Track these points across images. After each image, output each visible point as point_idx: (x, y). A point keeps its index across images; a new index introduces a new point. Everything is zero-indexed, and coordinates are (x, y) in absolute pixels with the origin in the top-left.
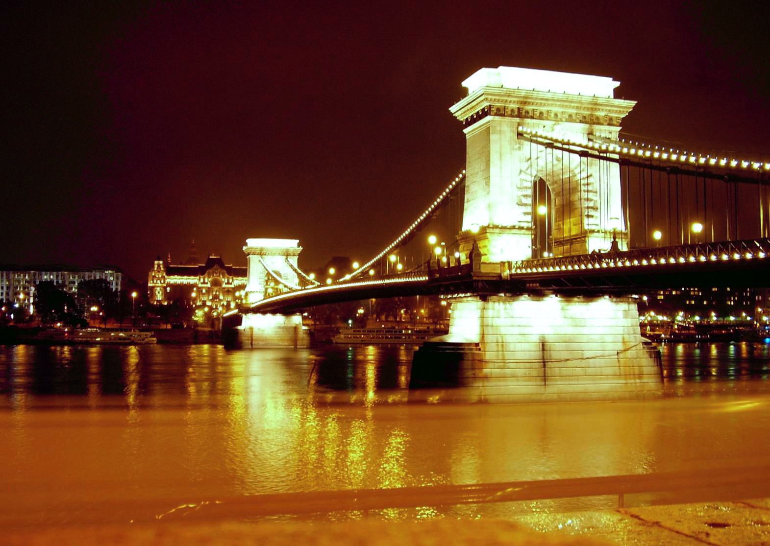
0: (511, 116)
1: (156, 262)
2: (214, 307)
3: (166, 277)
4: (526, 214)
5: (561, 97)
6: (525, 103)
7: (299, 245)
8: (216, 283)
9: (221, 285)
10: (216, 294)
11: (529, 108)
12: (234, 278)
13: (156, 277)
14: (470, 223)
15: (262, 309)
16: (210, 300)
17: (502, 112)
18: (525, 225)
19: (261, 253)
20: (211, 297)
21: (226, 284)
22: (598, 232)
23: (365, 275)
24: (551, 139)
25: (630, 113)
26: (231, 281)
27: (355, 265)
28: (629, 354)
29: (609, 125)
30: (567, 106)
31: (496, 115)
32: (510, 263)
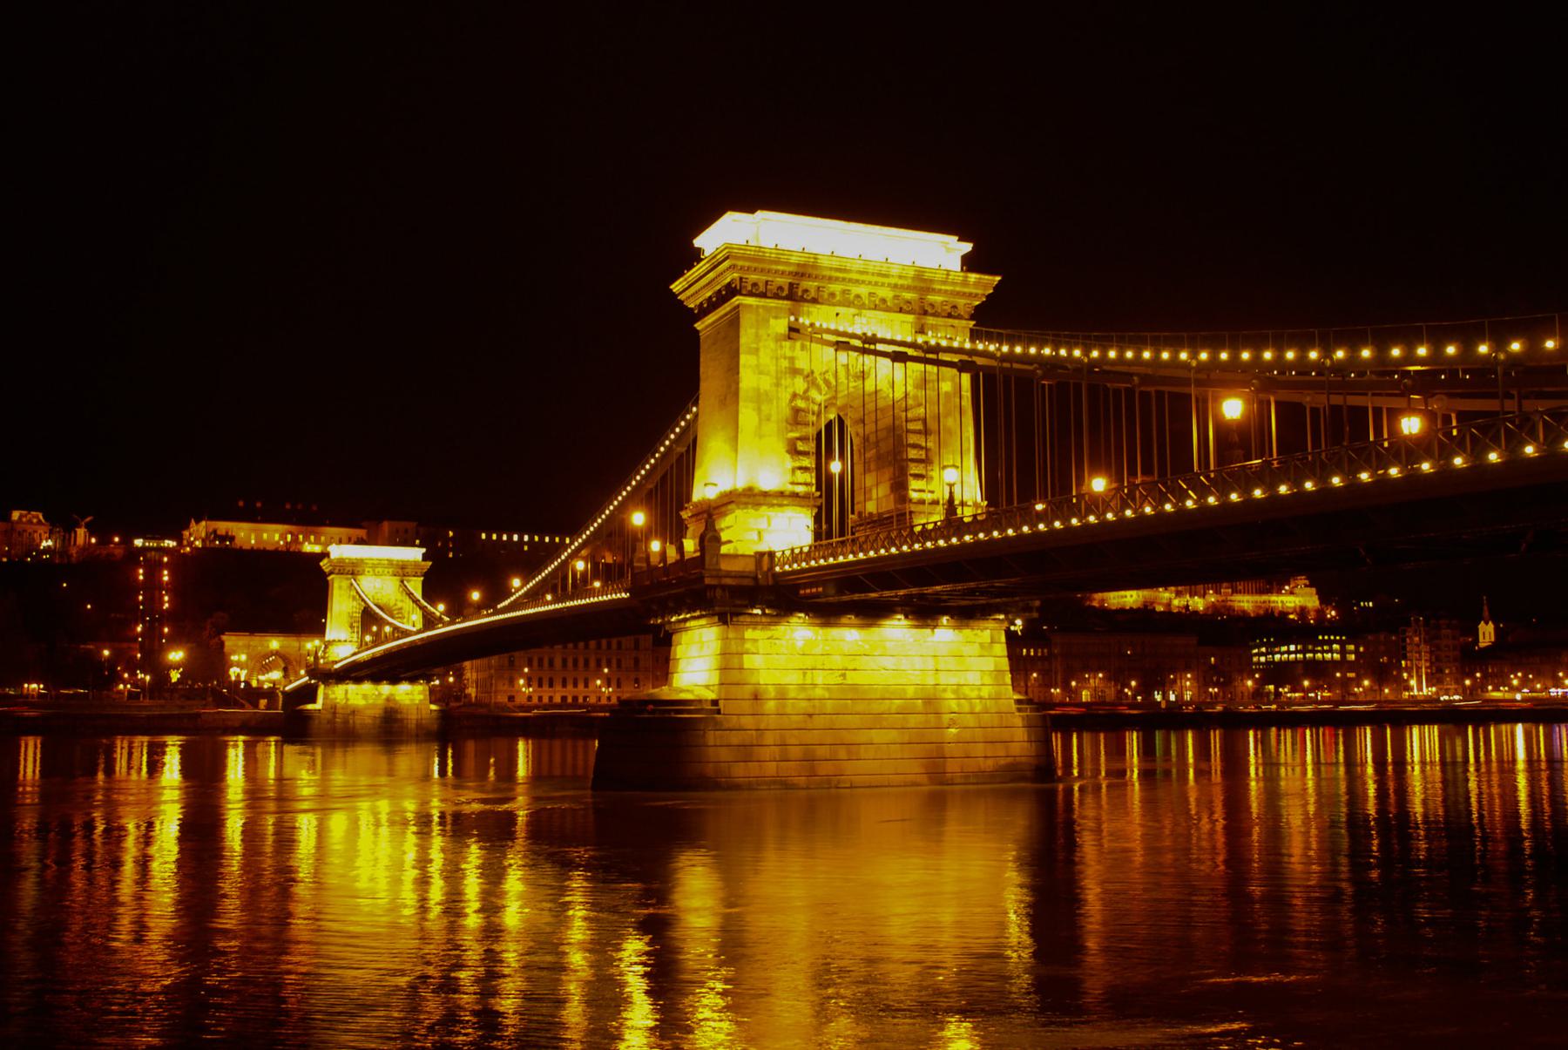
0: (776, 296)
4: (805, 469)
6: (803, 275)
7: (425, 557)
11: (811, 285)
14: (708, 484)
15: (353, 673)
17: (762, 289)
18: (801, 489)
19: (352, 570)
23: (534, 596)
24: (844, 334)
25: (988, 297)
27: (516, 582)
30: (876, 284)
31: (751, 294)
32: (771, 555)
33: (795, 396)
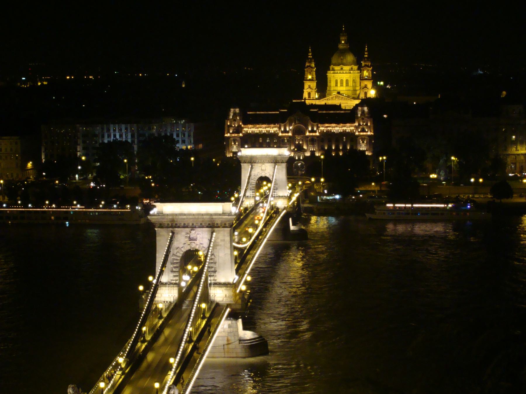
0: (168, 227)
1: (232, 110)
2: (297, 158)
3: (242, 126)
5: (191, 217)
8: (298, 132)
9: (304, 133)
10: (299, 143)
12: (319, 125)
13: (232, 126)
16: (293, 151)
19: (252, 161)
21: (310, 132)
22: (215, 284)
26: (315, 129)
28: (230, 346)
29: (224, 227)
31: (159, 227)
33: (174, 255)
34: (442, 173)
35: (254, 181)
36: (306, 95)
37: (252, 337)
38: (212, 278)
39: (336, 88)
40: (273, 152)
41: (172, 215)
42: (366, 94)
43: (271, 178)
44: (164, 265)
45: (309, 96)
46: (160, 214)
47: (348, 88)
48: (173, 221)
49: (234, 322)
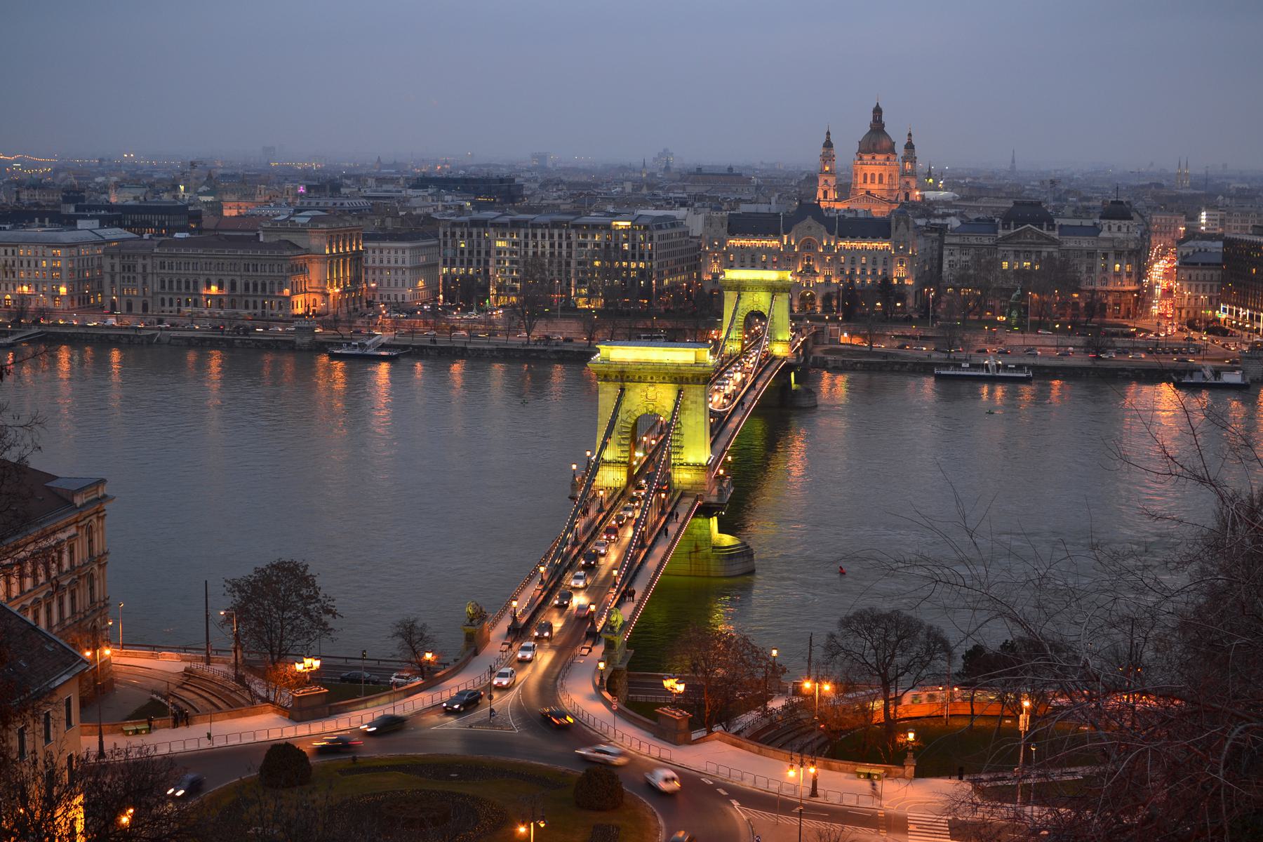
0: (616, 381)
19: (740, 287)
20: (800, 269)
34: (1015, 314)
35: (740, 318)
36: (820, 195)
37: (731, 543)
38: (677, 456)
39: (864, 186)
40: (771, 275)
41: (622, 363)
42: (907, 195)
43: (766, 314)
44: (608, 435)
45: (825, 197)
46: (606, 360)
47: (881, 187)
48: (622, 372)
49: (705, 520)
